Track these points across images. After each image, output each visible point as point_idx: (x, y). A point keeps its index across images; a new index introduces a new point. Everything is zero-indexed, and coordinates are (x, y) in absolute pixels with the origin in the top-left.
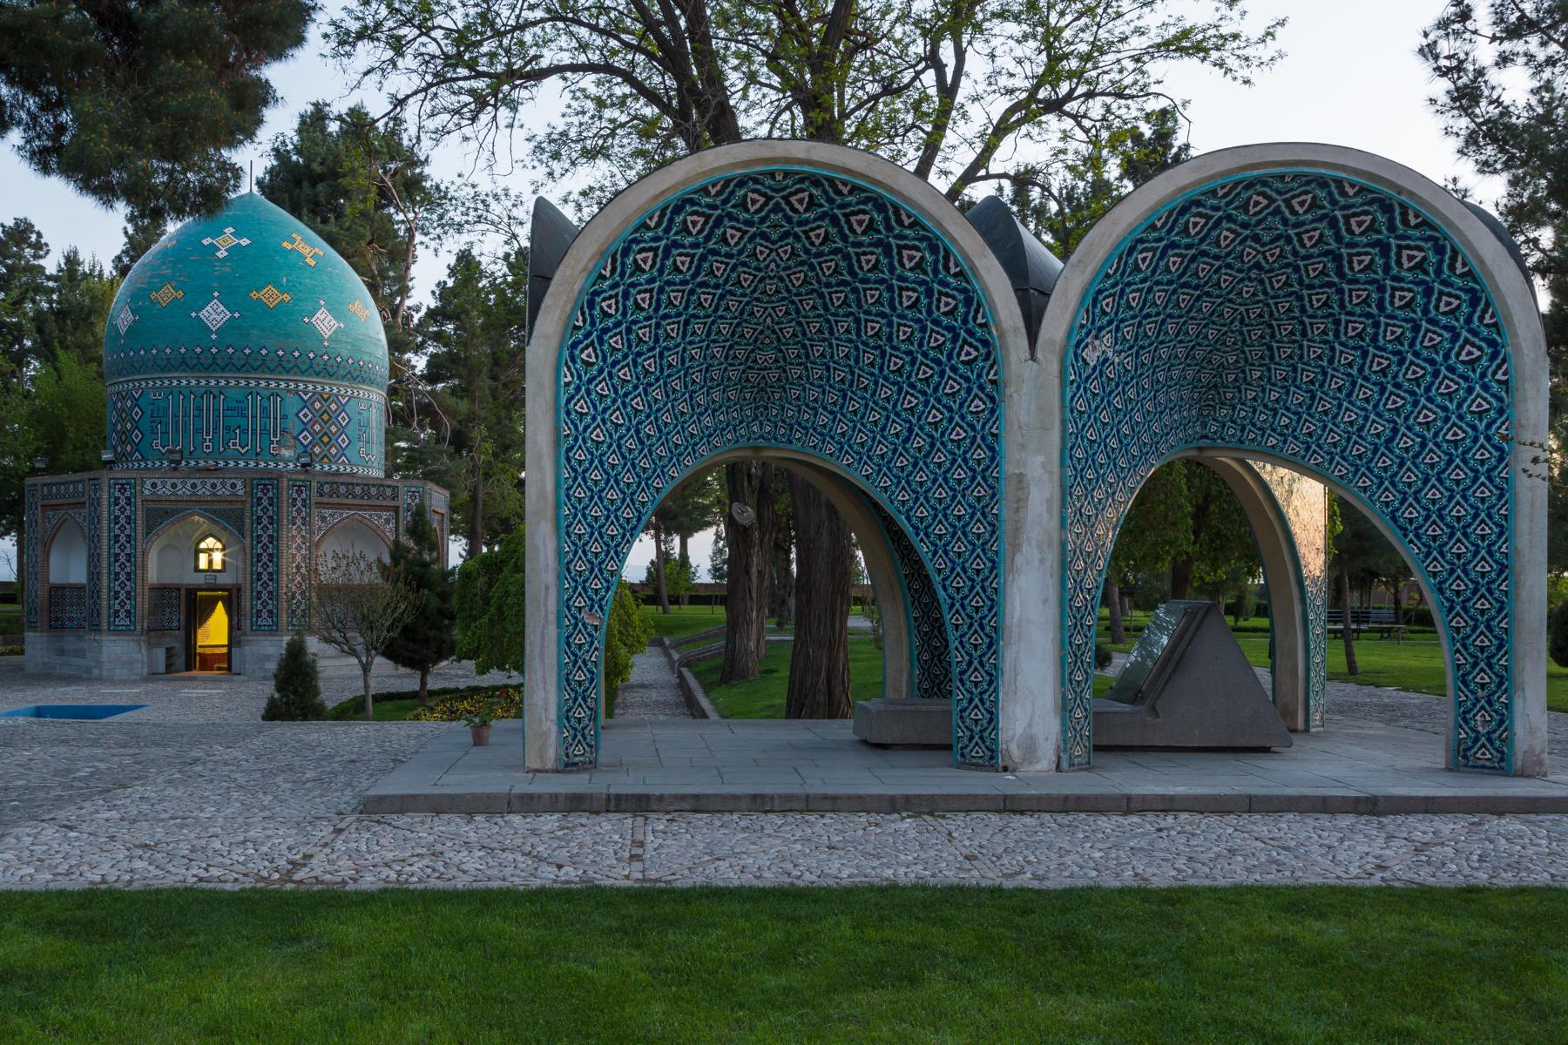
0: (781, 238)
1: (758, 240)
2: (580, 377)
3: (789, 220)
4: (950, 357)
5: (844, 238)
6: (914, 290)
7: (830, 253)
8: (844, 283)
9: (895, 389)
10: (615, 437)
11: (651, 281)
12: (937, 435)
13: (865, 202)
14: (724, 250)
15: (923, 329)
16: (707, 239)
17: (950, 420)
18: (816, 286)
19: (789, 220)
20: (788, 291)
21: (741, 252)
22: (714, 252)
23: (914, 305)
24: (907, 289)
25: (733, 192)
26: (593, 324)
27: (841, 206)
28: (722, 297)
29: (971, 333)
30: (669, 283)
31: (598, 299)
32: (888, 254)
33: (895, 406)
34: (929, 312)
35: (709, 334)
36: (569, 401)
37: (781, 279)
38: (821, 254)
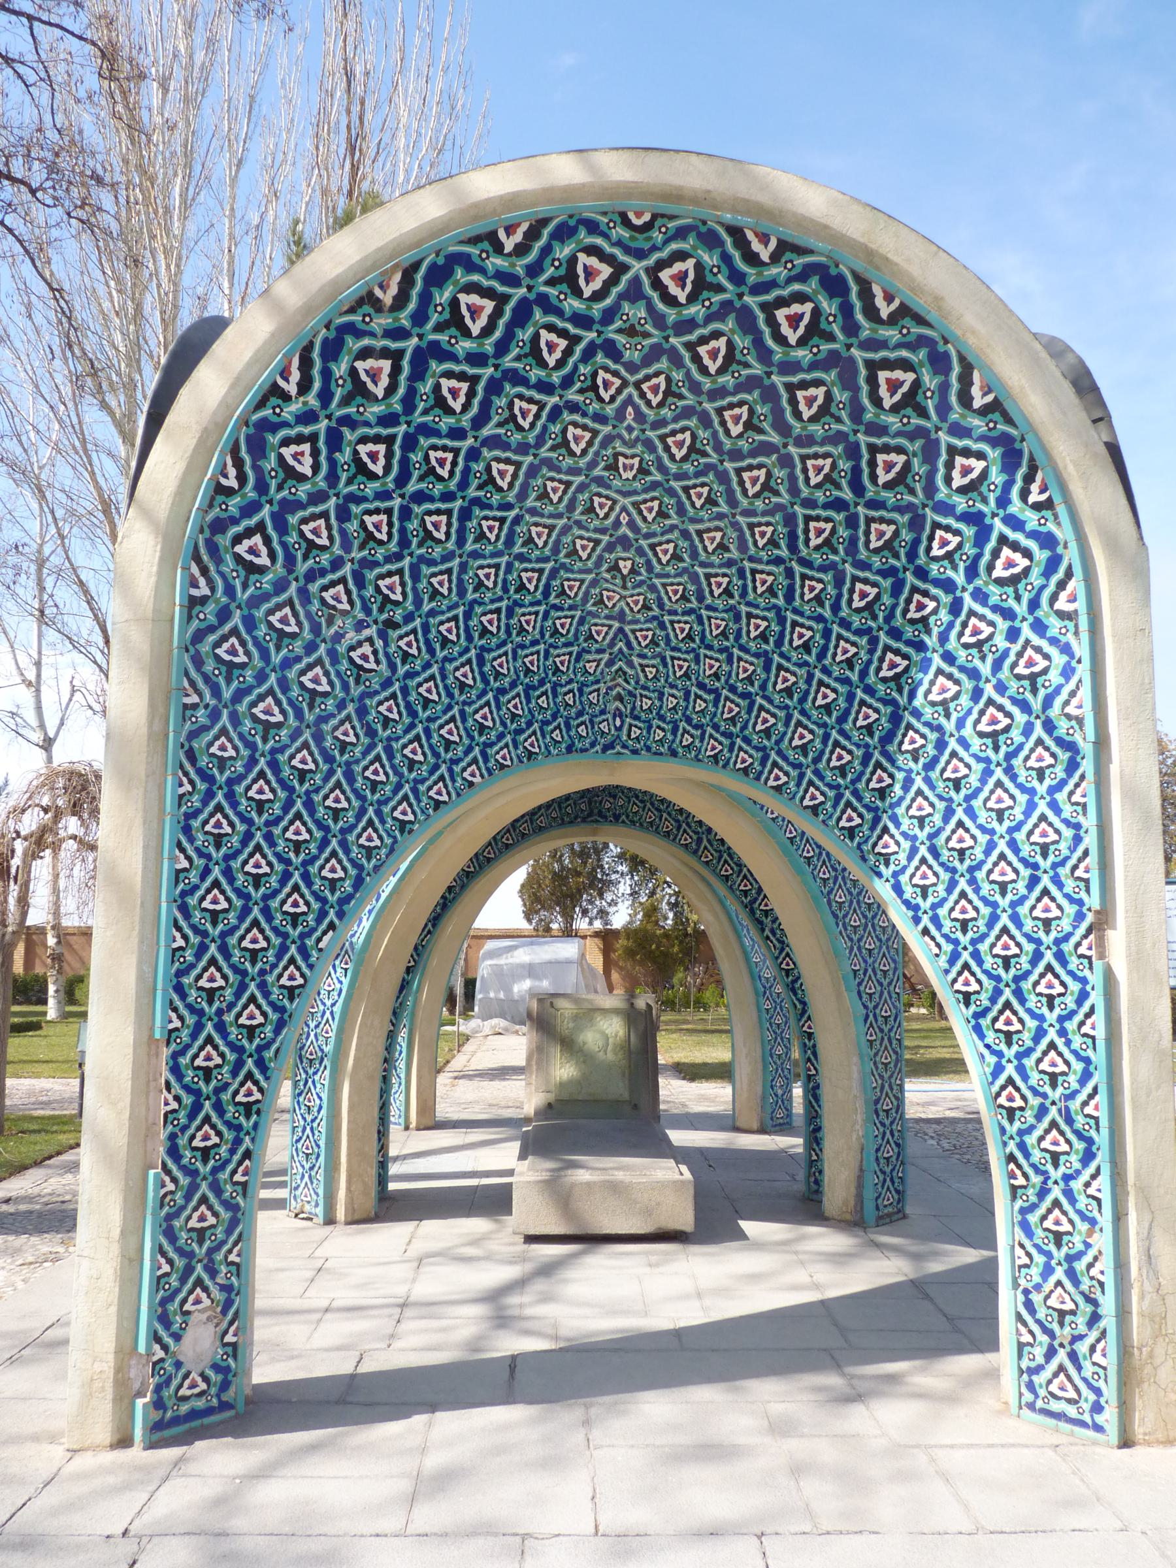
1: (600, 358)
2: (230, 591)
3: (659, 320)
6: (900, 450)
7: (739, 388)
8: (766, 449)
9: (863, 641)
10: (310, 717)
11: (389, 420)
13: (802, 277)
14: (535, 374)
16: (502, 348)
17: (977, 694)
18: (714, 458)
19: (659, 320)
20: (662, 469)
21: (567, 382)
22: (517, 378)
23: (901, 479)
24: (887, 449)
25: (547, 250)
26: (262, 487)
27: (756, 290)
28: (533, 471)
30: (428, 430)
31: (274, 439)
33: (864, 674)
35: (509, 542)
36: (198, 637)
37: (649, 446)
38: (721, 392)
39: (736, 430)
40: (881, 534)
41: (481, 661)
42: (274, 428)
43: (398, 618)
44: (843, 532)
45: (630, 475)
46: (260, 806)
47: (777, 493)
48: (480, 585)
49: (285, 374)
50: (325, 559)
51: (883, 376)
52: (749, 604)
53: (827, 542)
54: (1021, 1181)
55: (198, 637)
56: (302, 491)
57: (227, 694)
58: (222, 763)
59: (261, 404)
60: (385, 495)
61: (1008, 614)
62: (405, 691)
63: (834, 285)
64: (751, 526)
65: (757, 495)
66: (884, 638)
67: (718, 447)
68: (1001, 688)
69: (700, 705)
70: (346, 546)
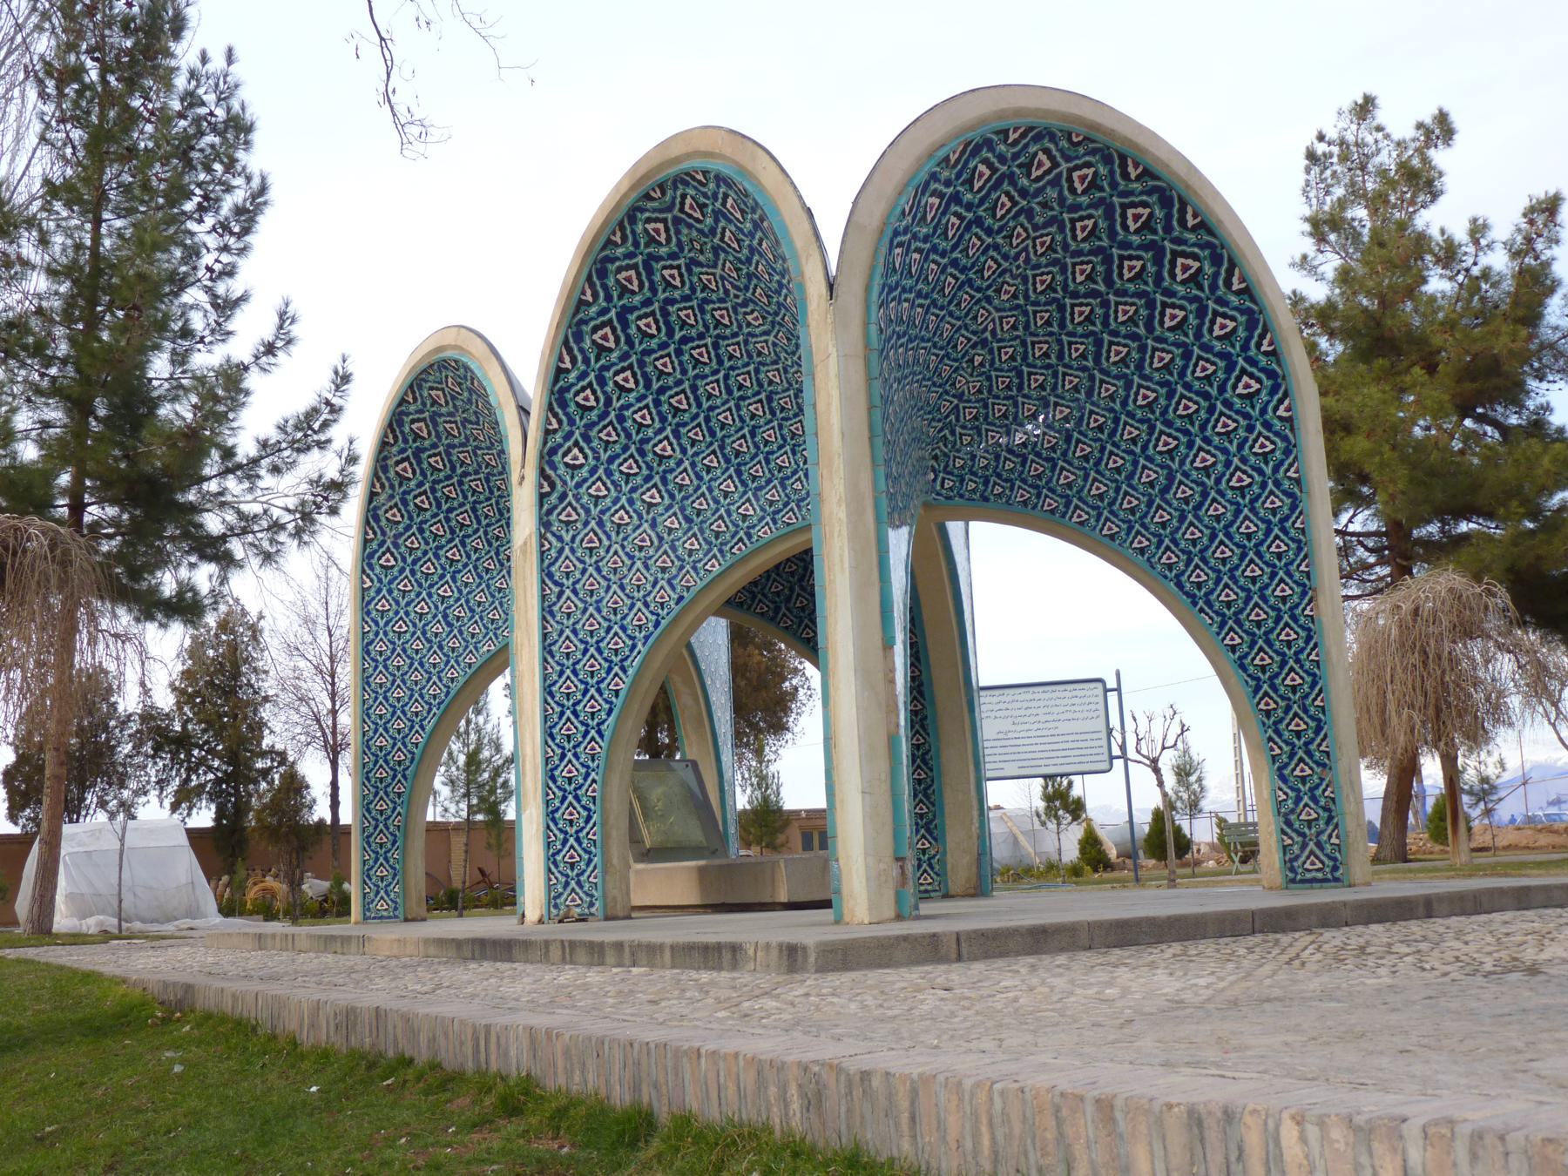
0: (1047, 224)
4: (1222, 389)
5: (1112, 234)
6: (1182, 308)
7: (1091, 253)
8: (1094, 294)
9: (1145, 427)
12: (1210, 482)
13: (1149, 193)
15: (1187, 356)
17: (1228, 464)
18: (1060, 295)
23: (1180, 327)
24: (1173, 306)
29: (1252, 362)
32: (1158, 261)
34: (1198, 335)
37: (1025, 280)
39: (1080, 278)
40: (1161, 359)
44: (1135, 355)
45: (1005, 297)
47: (1094, 324)
51: (1180, 261)
52: (1057, 396)
53: (1123, 360)
54: (1278, 751)
61: (1247, 416)
63: (1166, 202)
64: (1070, 344)
65: (1080, 324)
66: (1159, 426)
67: (1065, 287)
68: (1244, 460)
69: (1009, 465)
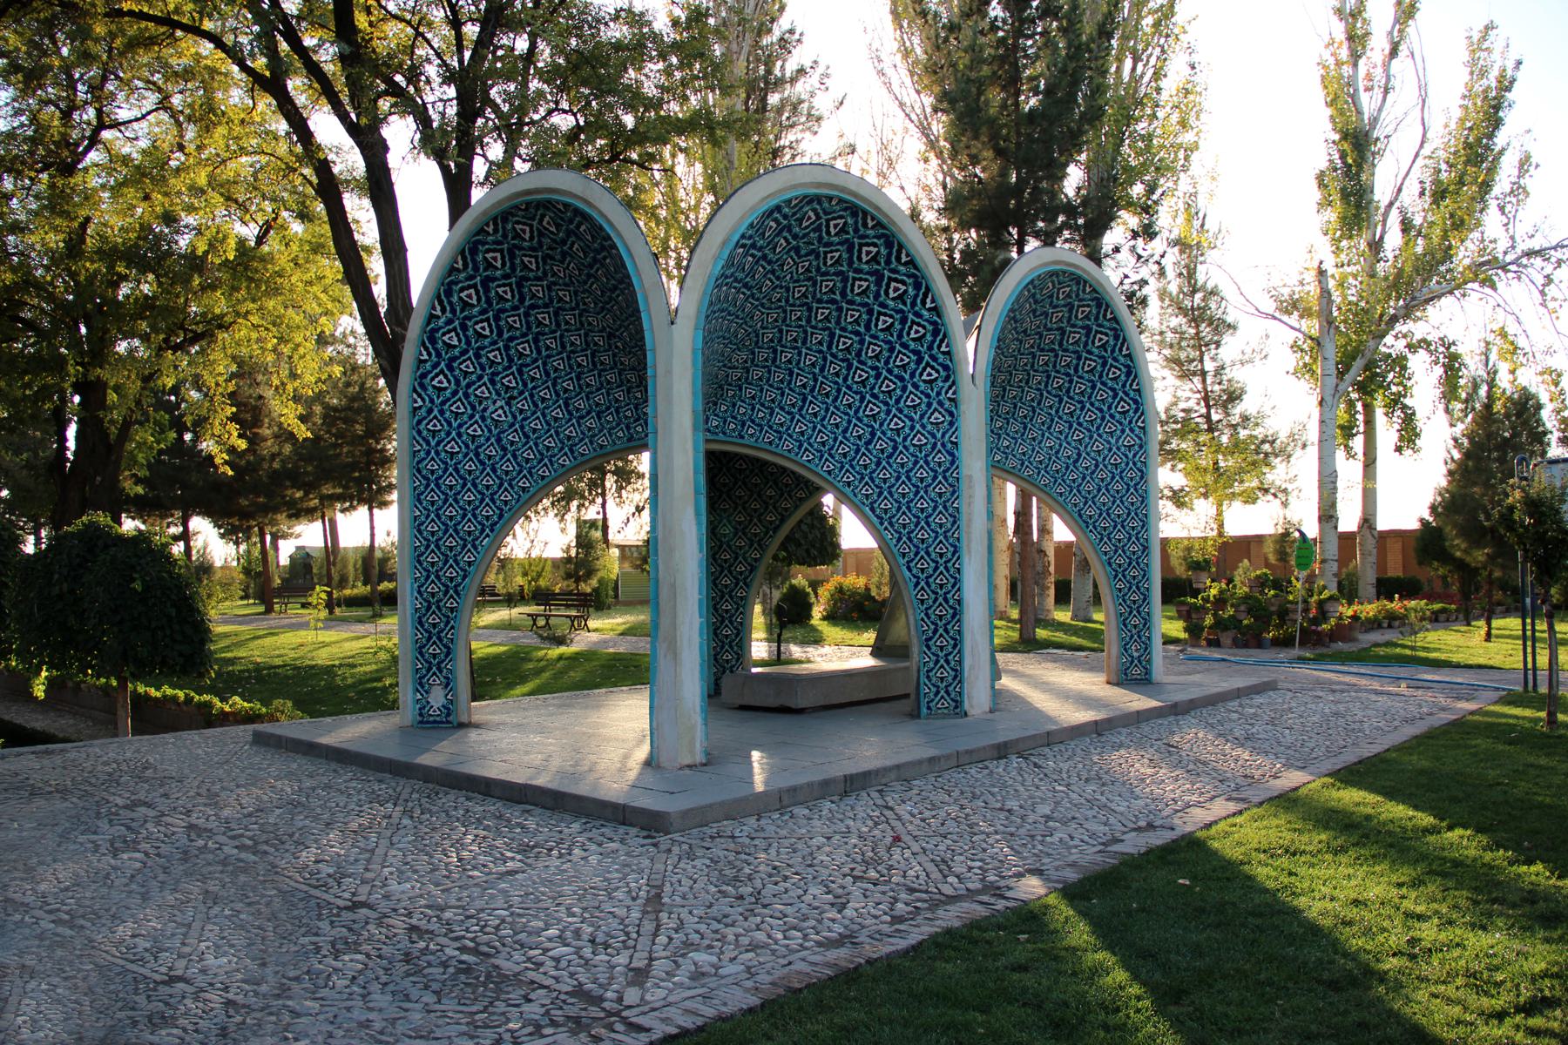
2: (432, 401)
26: (439, 355)
31: (438, 335)
36: (419, 422)
41: (567, 405)
42: (437, 330)
43: (515, 393)
46: (451, 488)
48: (556, 370)
49: (434, 308)
50: (474, 377)
55: (419, 422)
56: (456, 352)
57: (433, 443)
58: (433, 472)
59: (428, 323)
60: (495, 343)
62: (522, 427)
70: (483, 369)
